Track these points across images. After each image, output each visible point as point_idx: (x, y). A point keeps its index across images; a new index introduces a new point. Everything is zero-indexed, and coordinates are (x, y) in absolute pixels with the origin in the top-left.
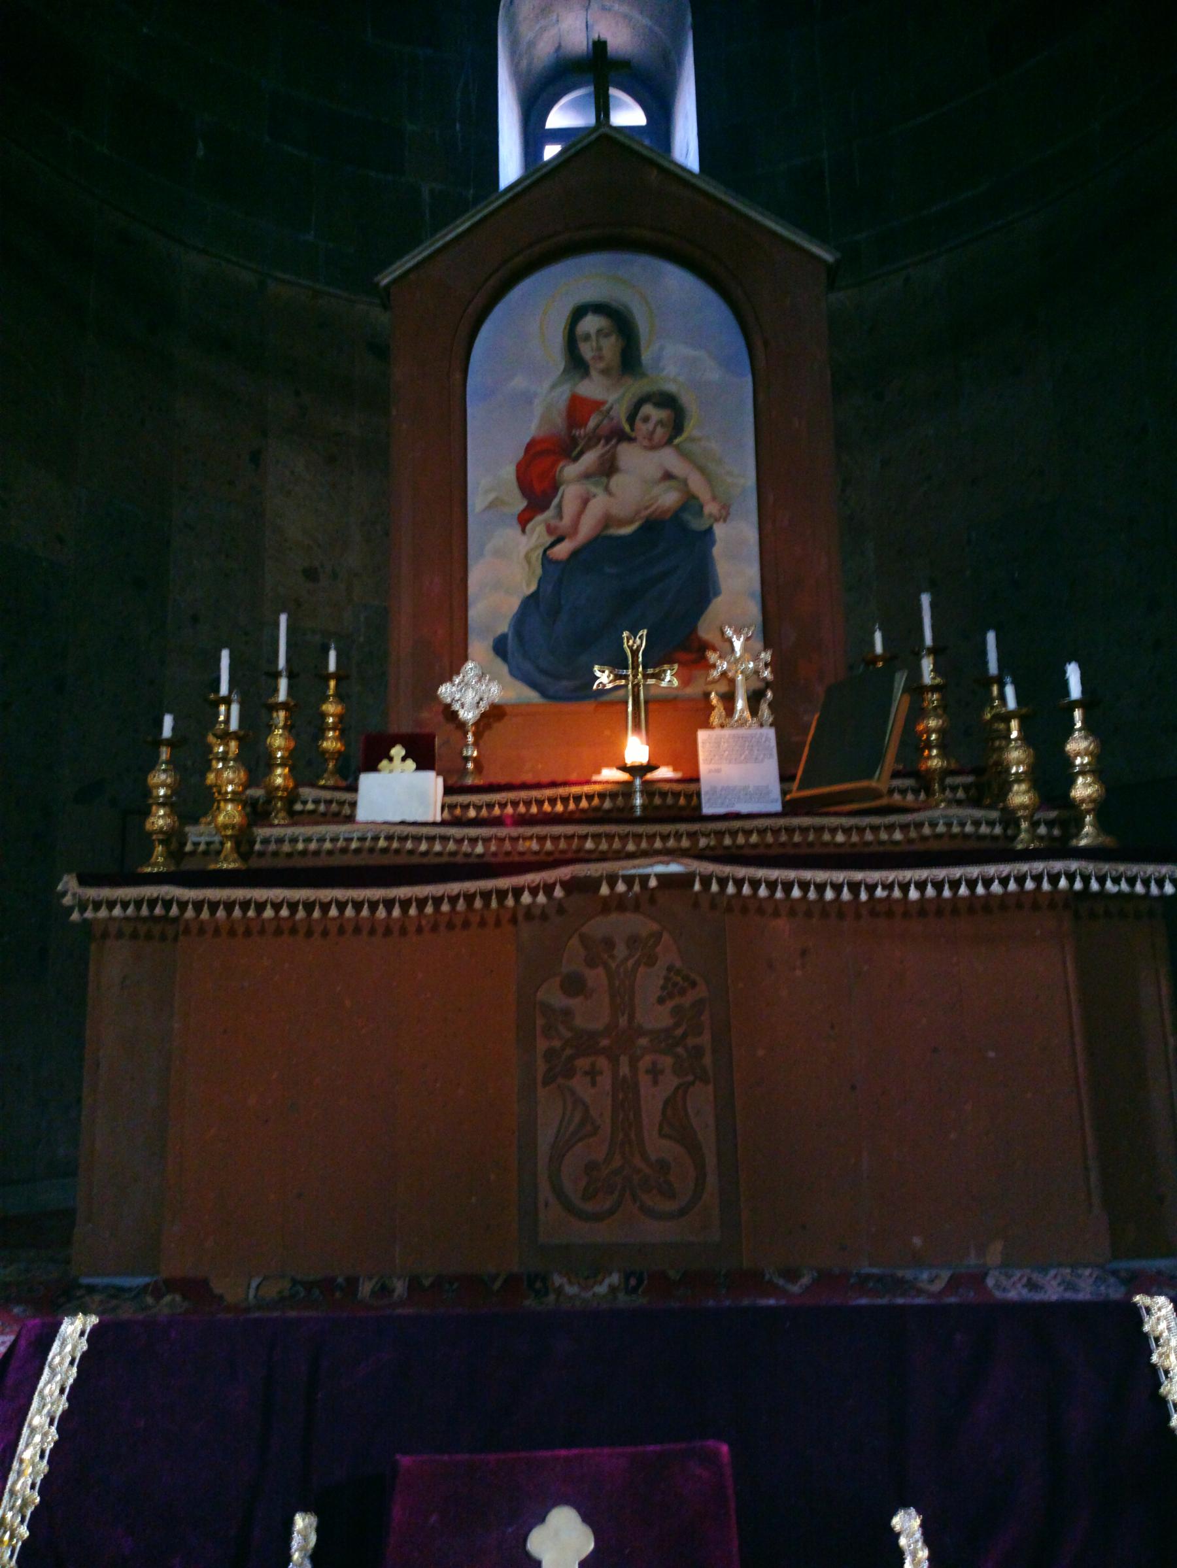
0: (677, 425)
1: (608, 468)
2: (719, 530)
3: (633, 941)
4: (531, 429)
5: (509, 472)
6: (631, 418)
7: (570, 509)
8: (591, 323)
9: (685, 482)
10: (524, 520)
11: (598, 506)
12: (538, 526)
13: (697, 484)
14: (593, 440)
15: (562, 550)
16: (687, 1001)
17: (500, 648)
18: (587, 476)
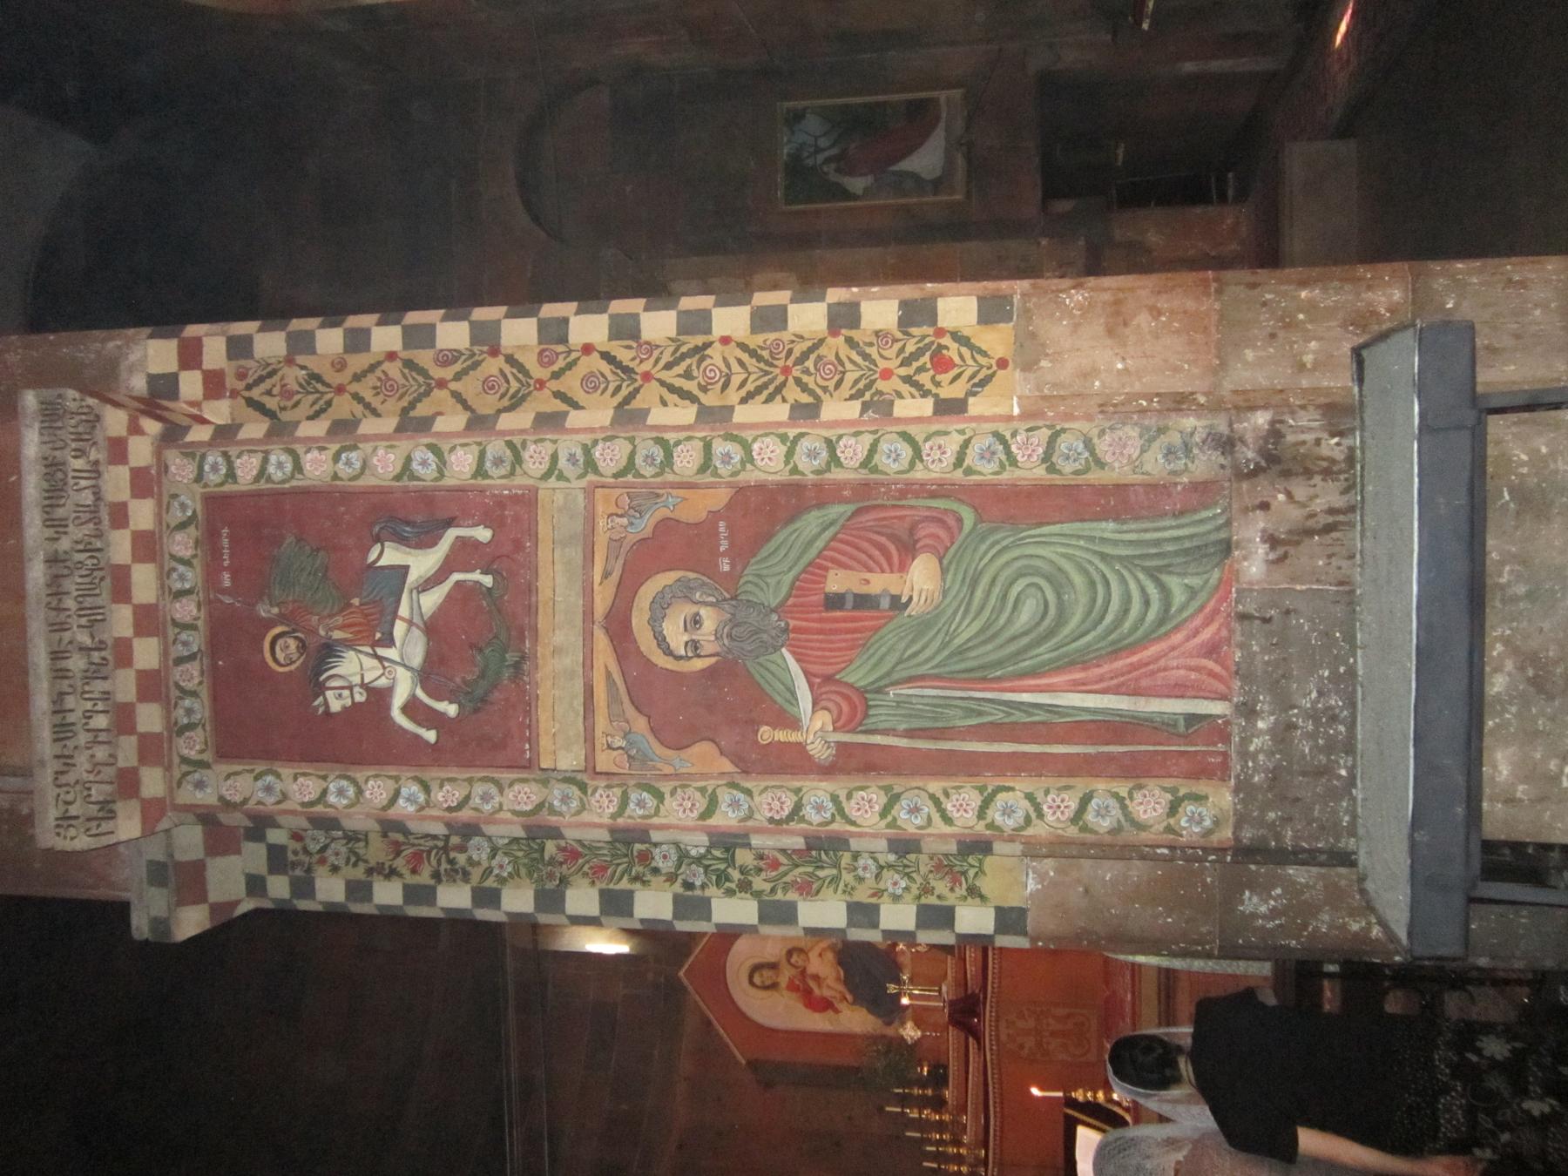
0: (801, 951)
1: (816, 978)
4: (800, 1007)
5: (817, 1016)
6: (796, 967)
8: (757, 980)
10: (837, 1011)
11: (831, 981)
12: (838, 1005)
14: (805, 983)
15: (849, 997)
16: (1026, 1012)
17: (889, 1024)
18: (820, 986)
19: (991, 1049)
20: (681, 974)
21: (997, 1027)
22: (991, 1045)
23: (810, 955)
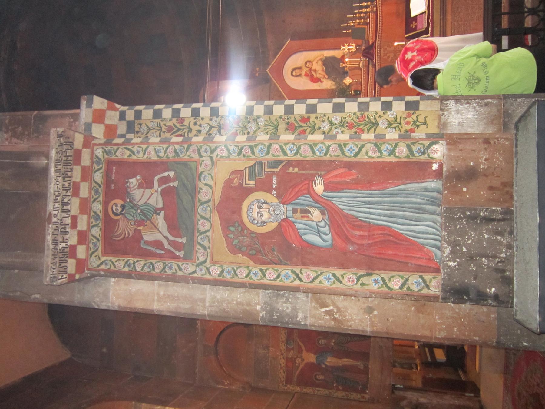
0: (310, 61)
1: (315, 71)
2: (325, 56)
3: (384, 51)
4: (309, 81)
5: (315, 84)
6: (308, 68)
7: (320, 76)
8: (294, 74)
9: (318, 60)
10: (322, 82)
11: (320, 72)
13: (318, 59)
14: (311, 73)
15: (327, 77)
18: (316, 74)
19: (378, 56)
20: (268, 71)
21: (380, 50)
22: (378, 54)
23: (313, 63)
